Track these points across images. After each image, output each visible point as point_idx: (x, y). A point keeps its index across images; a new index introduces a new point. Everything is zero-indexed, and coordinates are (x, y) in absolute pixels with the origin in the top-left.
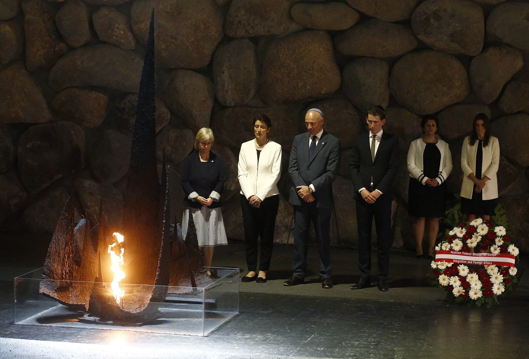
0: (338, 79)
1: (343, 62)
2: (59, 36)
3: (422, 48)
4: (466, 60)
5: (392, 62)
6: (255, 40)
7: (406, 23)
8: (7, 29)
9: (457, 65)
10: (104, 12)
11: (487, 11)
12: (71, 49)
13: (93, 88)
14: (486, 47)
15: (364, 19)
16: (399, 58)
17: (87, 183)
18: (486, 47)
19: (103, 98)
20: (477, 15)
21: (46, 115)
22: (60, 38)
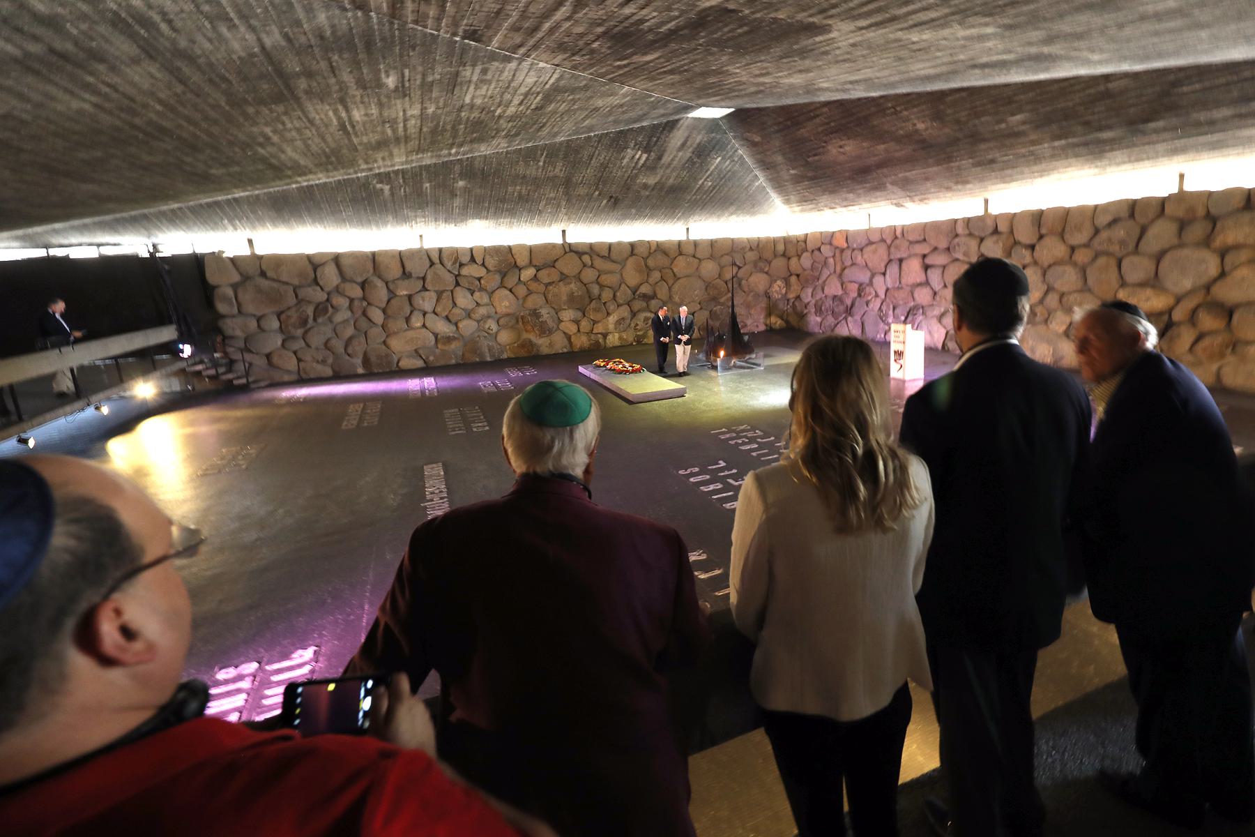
21: (840, 292)
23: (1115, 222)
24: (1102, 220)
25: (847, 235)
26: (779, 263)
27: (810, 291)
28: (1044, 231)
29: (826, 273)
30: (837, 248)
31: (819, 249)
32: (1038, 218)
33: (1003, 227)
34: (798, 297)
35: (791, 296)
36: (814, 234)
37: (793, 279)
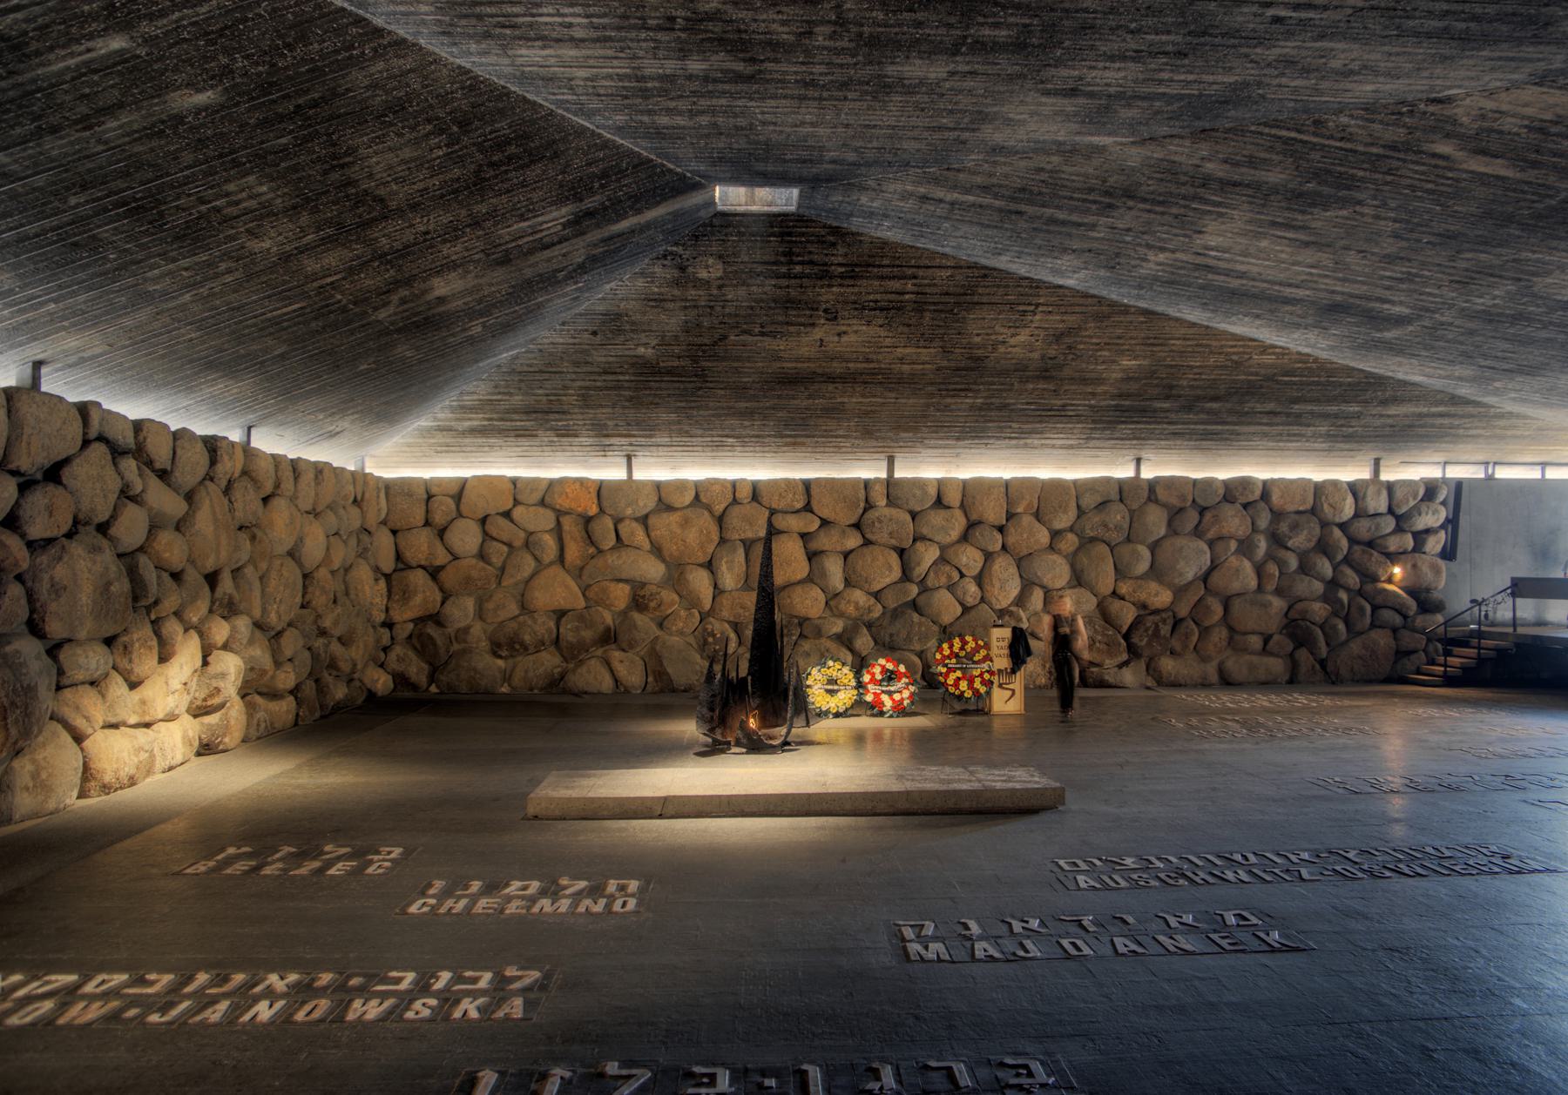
0: (807, 570)
1: (812, 556)
2: (590, 539)
3: (868, 543)
4: (901, 552)
5: (846, 555)
7: (857, 526)
13: (620, 581)
15: (825, 523)
16: (851, 551)
19: (627, 588)
20: (909, 518)
23: (1102, 505)
24: (1089, 501)
25: (600, 488)
27: (469, 604)
30: (560, 513)
33: (953, 498)
34: (436, 619)
35: (404, 615)
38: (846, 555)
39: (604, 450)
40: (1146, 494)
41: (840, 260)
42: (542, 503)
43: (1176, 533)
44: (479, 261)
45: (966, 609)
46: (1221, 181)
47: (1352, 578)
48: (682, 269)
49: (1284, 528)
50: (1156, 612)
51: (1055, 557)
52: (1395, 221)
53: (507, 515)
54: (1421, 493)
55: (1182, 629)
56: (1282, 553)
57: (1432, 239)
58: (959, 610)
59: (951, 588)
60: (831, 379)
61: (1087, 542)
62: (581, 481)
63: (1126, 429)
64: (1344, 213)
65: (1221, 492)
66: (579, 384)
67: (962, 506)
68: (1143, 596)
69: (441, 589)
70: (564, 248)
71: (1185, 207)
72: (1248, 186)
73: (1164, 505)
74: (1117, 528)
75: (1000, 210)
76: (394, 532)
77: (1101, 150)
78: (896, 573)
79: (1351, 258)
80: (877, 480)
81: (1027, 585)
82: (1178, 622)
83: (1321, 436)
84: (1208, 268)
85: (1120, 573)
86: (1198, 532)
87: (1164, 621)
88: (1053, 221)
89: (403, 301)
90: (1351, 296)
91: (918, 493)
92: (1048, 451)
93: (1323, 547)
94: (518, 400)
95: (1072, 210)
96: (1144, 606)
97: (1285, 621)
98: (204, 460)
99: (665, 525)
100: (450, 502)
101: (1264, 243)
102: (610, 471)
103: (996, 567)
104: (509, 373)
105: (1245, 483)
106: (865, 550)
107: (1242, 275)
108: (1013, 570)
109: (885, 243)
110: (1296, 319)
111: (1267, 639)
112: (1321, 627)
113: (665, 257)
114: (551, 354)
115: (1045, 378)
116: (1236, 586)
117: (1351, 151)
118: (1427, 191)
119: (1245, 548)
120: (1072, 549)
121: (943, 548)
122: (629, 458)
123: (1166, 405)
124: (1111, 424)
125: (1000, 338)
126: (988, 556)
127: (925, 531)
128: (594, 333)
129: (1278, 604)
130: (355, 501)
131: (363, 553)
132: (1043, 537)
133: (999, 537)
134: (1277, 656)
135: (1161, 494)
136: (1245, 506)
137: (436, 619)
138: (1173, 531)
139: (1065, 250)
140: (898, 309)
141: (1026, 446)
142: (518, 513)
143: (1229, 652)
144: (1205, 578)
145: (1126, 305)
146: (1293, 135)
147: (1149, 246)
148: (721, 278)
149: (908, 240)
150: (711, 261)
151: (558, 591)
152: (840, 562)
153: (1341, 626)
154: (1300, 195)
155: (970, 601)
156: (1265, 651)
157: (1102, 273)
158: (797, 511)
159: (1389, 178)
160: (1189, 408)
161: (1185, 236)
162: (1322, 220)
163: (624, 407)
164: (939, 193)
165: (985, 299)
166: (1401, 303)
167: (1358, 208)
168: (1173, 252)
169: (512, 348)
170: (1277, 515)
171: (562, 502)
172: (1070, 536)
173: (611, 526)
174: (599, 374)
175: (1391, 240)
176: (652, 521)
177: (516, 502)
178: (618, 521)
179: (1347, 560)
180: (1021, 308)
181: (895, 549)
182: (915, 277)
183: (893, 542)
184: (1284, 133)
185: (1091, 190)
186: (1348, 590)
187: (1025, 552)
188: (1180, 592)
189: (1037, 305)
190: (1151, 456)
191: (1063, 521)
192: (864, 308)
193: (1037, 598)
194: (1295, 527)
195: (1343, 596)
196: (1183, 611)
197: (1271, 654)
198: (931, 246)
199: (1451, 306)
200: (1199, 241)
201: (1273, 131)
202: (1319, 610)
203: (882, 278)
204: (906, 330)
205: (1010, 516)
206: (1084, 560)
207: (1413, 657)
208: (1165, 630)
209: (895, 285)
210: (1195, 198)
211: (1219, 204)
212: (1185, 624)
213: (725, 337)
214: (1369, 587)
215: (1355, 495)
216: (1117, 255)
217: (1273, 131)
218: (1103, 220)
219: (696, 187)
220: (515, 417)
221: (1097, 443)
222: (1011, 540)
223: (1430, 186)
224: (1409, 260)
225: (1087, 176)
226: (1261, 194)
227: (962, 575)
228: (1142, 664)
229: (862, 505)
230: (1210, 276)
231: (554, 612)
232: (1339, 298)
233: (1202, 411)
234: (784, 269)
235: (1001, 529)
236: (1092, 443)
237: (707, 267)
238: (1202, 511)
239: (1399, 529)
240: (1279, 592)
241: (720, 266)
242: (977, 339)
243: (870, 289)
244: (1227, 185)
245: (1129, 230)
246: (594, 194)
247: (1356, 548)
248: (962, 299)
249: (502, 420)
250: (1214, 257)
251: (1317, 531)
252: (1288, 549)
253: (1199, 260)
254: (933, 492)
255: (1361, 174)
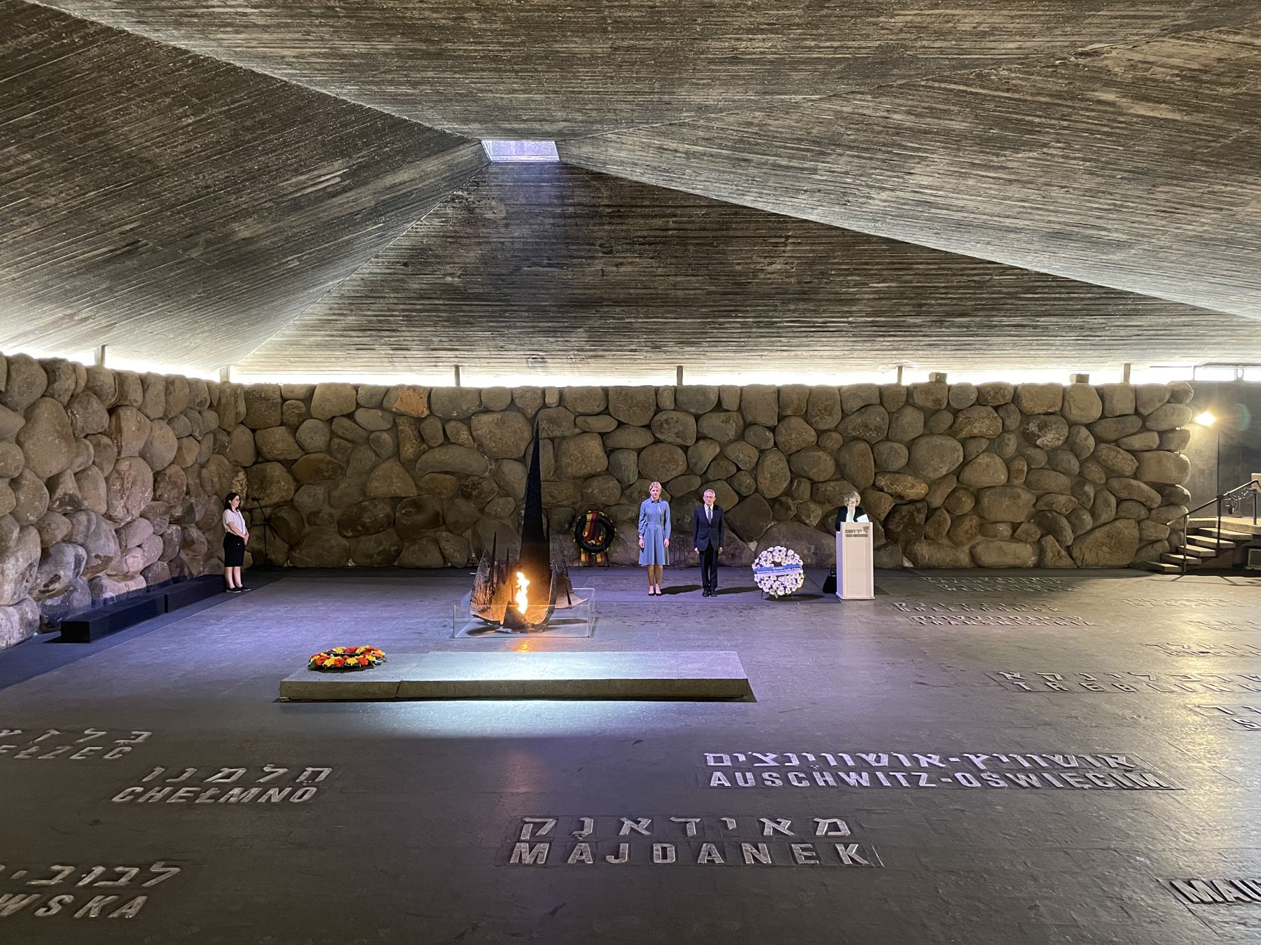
1: (609, 452)
3: (657, 441)
4: (685, 449)
5: (639, 451)
6: (552, 440)
7: (648, 427)
8: (385, 436)
9: (680, 451)
10: (453, 423)
11: (697, 418)
12: (431, 448)
14: (698, 439)
15: (620, 424)
17: (444, 534)
18: (698, 439)
21: (413, 492)
22: (423, 440)
24: (855, 404)
25: (430, 393)
26: (242, 436)
28: (789, 413)
29: (365, 456)
31: (350, 416)
32: (779, 395)
33: (730, 403)
36: (334, 390)
37: (276, 470)
38: (639, 451)
39: (436, 362)
40: (904, 399)
41: (606, 202)
42: (380, 406)
43: (932, 434)
44: (271, 208)
45: (742, 498)
46: (910, 129)
47: (1095, 473)
48: (471, 211)
49: (1033, 427)
50: (912, 502)
51: (820, 453)
52: (1084, 160)
53: (350, 416)
54: (1167, 396)
55: (935, 518)
56: (1031, 451)
57: (1126, 175)
58: (737, 499)
59: (729, 480)
60: (617, 303)
61: (849, 440)
62: (414, 389)
63: (886, 342)
64: (1035, 154)
65: (974, 396)
66: (401, 307)
67: (740, 409)
68: (899, 489)
69: (295, 479)
70: (351, 195)
71: (888, 152)
72: (936, 133)
73: (920, 408)
74: (878, 429)
75: (728, 157)
76: (254, 431)
77: (797, 106)
78: (682, 467)
79: (1055, 192)
80: (667, 388)
81: (795, 476)
82: (931, 512)
83: (1069, 345)
84: (931, 205)
85: (880, 469)
86: (951, 432)
87: (918, 511)
88: (776, 166)
89: (209, 243)
90: (1067, 224)
91: (701, 398)
92: (818, 361)
93: (1070, 445)
94: (351, 320)
95: (791, 158)
96: (901, 497)
97: (1033, 510)
98: (42, 378)
99: (484, 424)
100: (302, 404)
101: (971, 182)
102: (439, 378)
103: (767, 463)
104: (340, 298)
105: (998, 389)
106: (656, 448)
107: (961, 209)
108: (784, 464)
109: (643, 187)
110: (1024, 245)
111: (1015, 527)
112: (1067, 517)
113: (453, 200)
114: (372, 282)
115: (804, 300)
116: (986, 480)
117: (1020, 100)
118: (1104, 133)
119: (995, 444)
120: (836, 446)
121: (723, 446)
122: (457, 367)
123: (918, 320)
124: (872, 337)
125: (759, 267)
126: (762, 452)
127: (706, 431)
128: (405, 265)
129: (1026, 497)
130: (211, 406)
131: (219, 449)
132: (811, 435)
133: (769, 434)
134: (1026, 542)
135: (918, 399)
136: (996, 408)
137: (290, 503)
138: (929, 431)
139: (798, 191)
140: (664, 243)
141: (796, 357)
142: (361, 415)
143: (979, 538)
144: (958, 473)
145: (868, 235)
146: (962, 88)
147: (871, 187)
148: (505, 218)
149: (661, 184)
150: (494, 203)
151: (390, 481)
152: (634, 456)
153: (1087, 517)
154: (989, 140)
155: (744, 491)
156: (1013, 538)
157: (837, 209)
158: (598, 414)
159: (1065, 123)
160: (940, 323)
161: (898, 177)
162: (1017, 160)
163: (445, 327)
164: (673, 145)
165: (739, 233)
166: (1117, 230)
167: (1045, 150)
168: (892, 190)
169: (336, 277)
170: (1026, 416)
171: (396, 406)
172: (835, 435)
173: (440, 426)
174: (417, 299)
175: (1087, 177)
176: (475, 421)
177: (358, 406)
178: (445, 421)
179: (1094, 456)
180: (773, 240)
181: (681, 447)
182: (675, 216)
183: (679, 441)
184: (953, 86)
185: (800, 140)
186: (1094, 484)
187: (794, 449)
188: (933, 484)
189: (787, 237)
190: (915, 365)
191: (828, 422)
192: (634, 243)
193: (805, 489)
194: (1042, 427)
195: (1089, 489)
196: (937, 501)
197: (1020, 541)
198: (683, 189)
199: (1165, 233)
200: (912, 180)
201: (943, 85)
202: (1062, 501)
203: (644, 216)
204: (674, 261)
205: (781, 418)
206: (845, 457)
207: (1157, 545)
208: (920, 518)
209: (658, 222)
210: (894, 145)
211: (918, 150)
212: (938, 513)
213: (518, 268)
214: (1115, 484)
215: (1102, 397)
216: (845, 194)
217: (943, 85)
218: (821, 165)
219: (462, 141)
220: (353, 333)
221: (861, 354)
222: (781, 439)
223: (1106, 129)
224: (1111, 194)
225: (790, 127)
226: (953, 141)
227: (739, 469)
228: (900, 547)
229: (653, 409)
230: (933, 210)
231: (392, 498)
232: (1057, 226)
233: (953, 325)
234: (559, 210)
235: (773, 429)
236: (856, 354)
237: (492, 208)
238: (956, 412)
239: (1144, 429)
240: (1028, 484)
241: (503, 208)
242: (739, 268)
243: (637, 226)
244: (916, 133)
245: (846, 173)
246: (360, 150)
247: (1103, 446)
248: (719, 233)
249: (342, 336)
250: (931, 195)
251: (1065, 431)
252: (1037, 447)
253: (918, 197)
254: (714, 398)
255: (1037, 120)
